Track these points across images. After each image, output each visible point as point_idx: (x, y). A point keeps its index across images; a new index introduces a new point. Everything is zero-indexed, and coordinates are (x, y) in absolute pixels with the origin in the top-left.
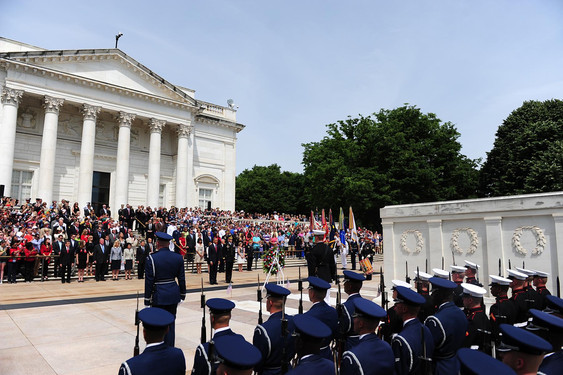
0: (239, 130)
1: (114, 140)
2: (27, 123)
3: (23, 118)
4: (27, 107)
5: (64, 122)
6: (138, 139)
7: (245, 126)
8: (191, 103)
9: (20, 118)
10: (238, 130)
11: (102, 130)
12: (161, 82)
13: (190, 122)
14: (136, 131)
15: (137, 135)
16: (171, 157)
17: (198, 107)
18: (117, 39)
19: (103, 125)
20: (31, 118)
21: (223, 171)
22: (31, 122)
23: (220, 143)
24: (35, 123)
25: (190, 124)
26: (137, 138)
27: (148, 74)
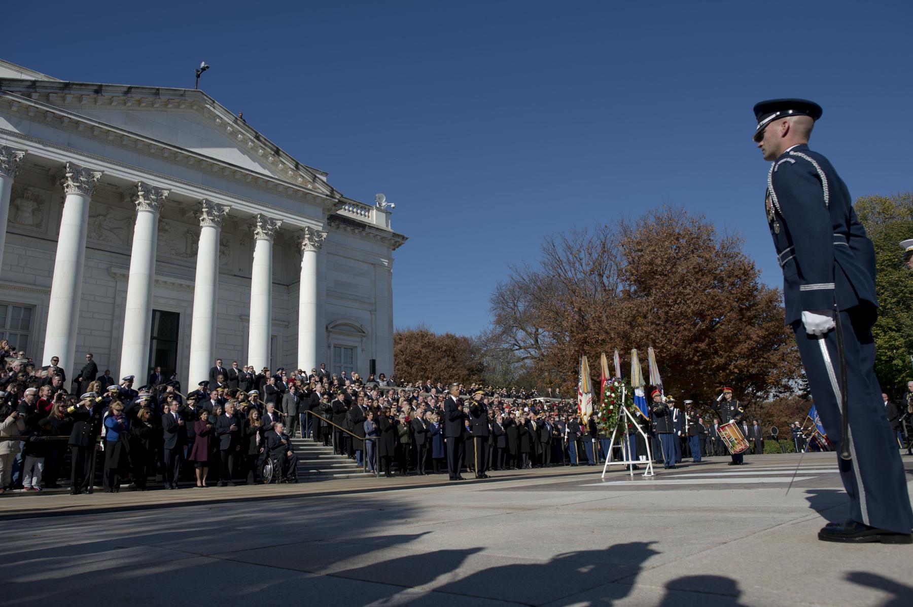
0: (398, 244)
1: (187, 254)
6: (229, 255)
7: (407, 238)
10: (396, 246)
12: (273, 153)
13: (322, 225)
15: (227, 248)
16: (286, 287)
17: (335, 198)
18: (198, 76)
19: (167, 227)
21: (371, 313)
25: (321, 228)
26: (226, 252)
27: (252, 138)
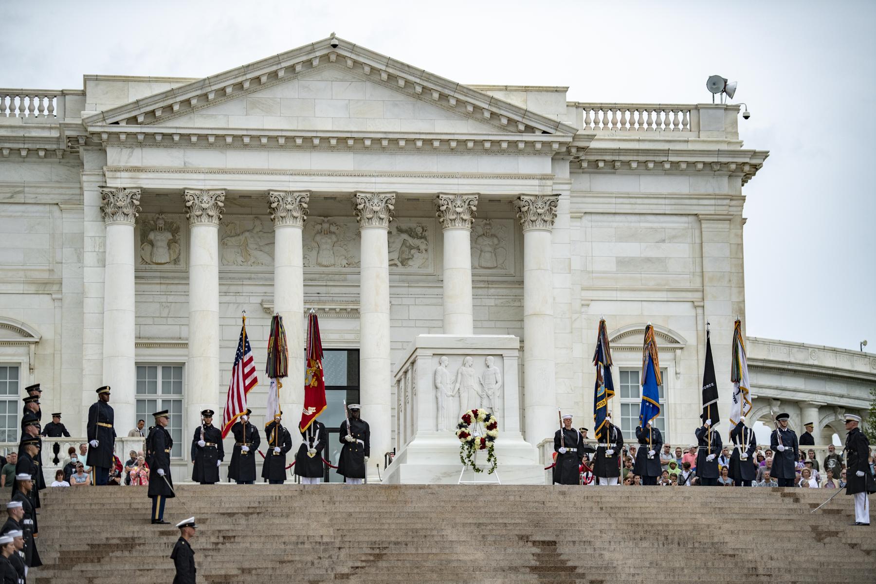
2: (162, 254)
3: (152, 244)
4: (157, 215)
5: (241, 237)
8: (544, 132)
9: (145, 243)
11: (329, 241)
14: (419, 230)
15: (423, 240)
19: (333, 229)
20: (169, 240)
21: (695, 307)
22: (169, 248)
23: (684, 219)
24: (177, 251)
26: (423, 247)
